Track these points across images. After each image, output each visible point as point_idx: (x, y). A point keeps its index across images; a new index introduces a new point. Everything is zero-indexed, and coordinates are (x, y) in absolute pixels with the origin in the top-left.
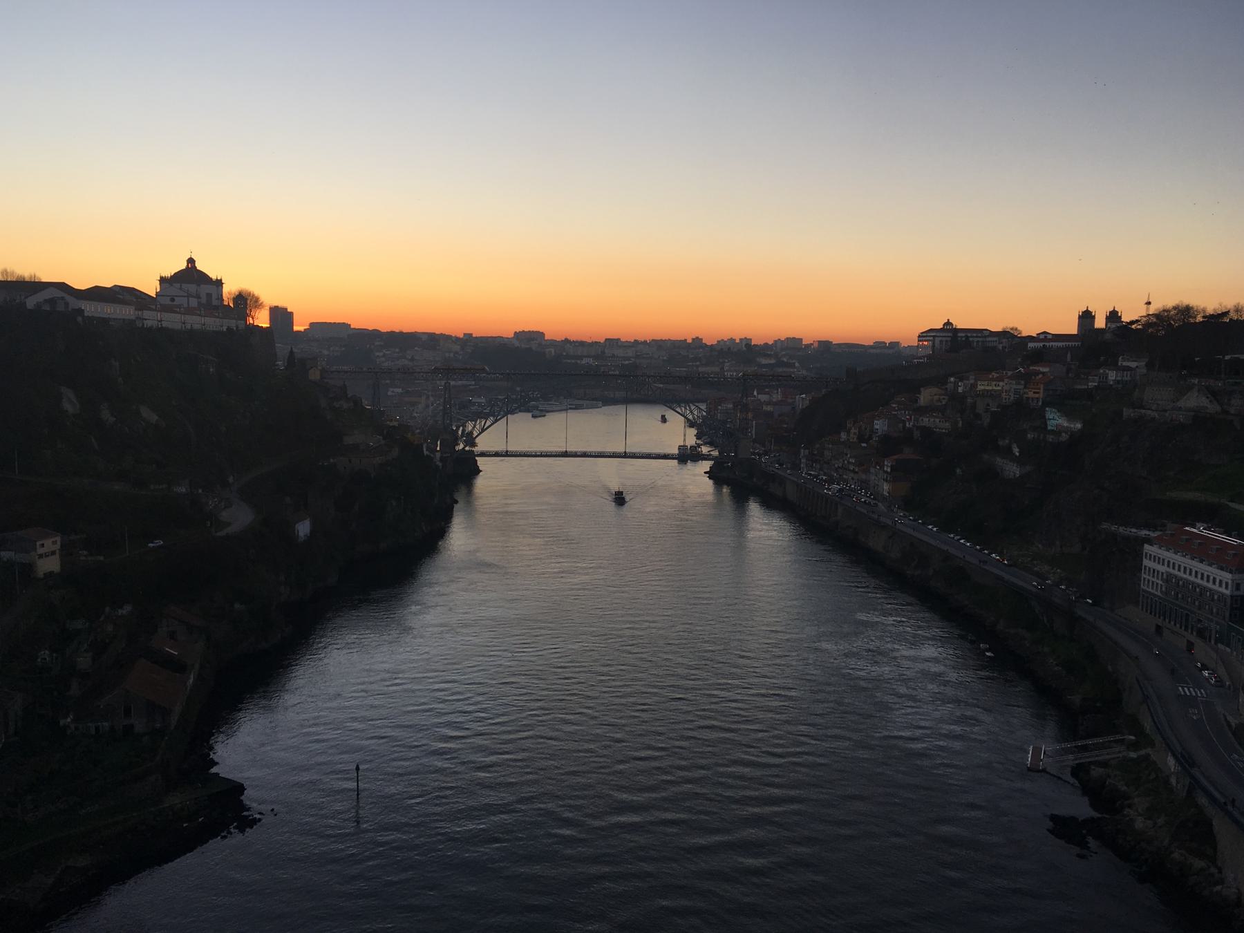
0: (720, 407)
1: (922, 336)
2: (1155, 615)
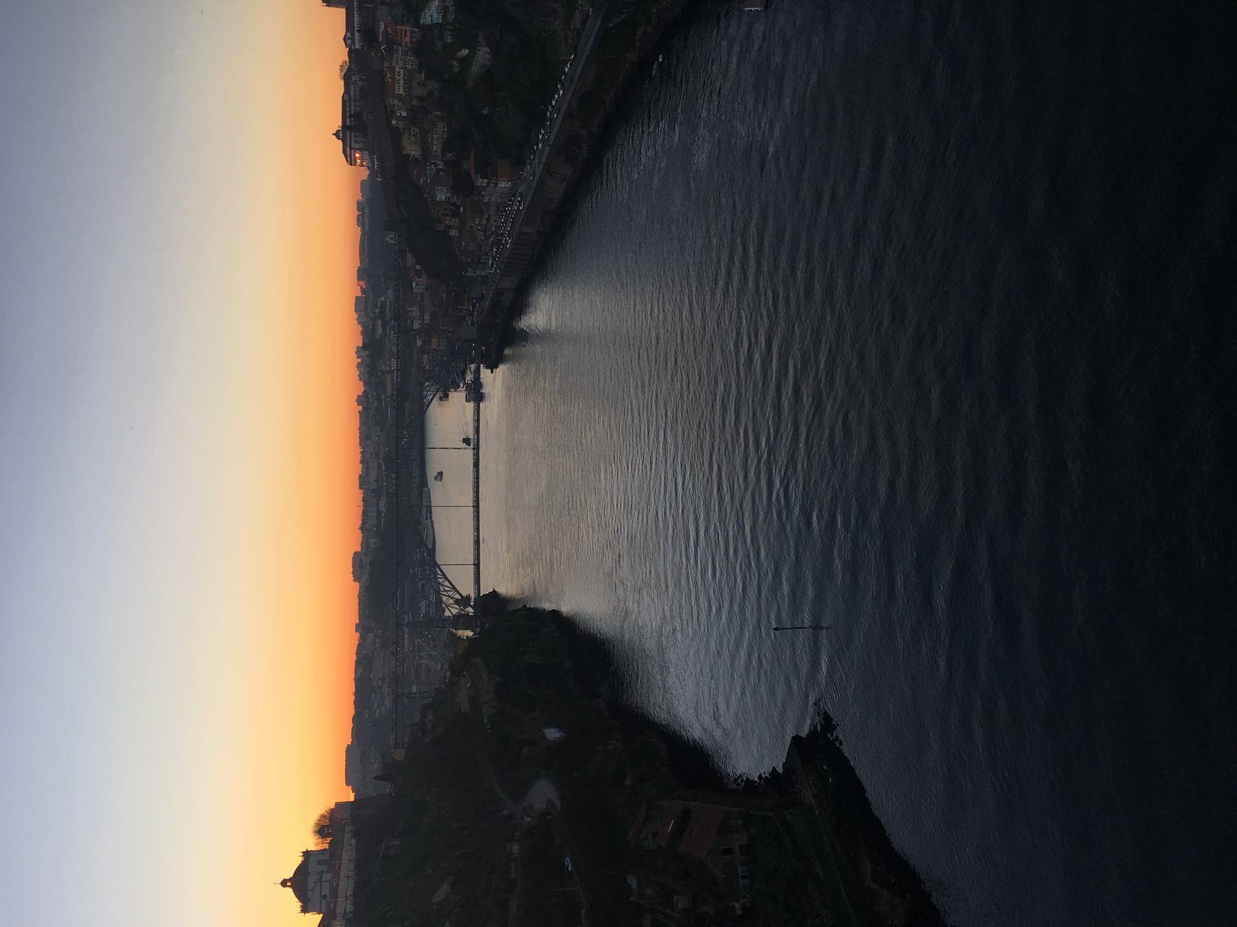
0: (427, 368)
1: (351, 161)
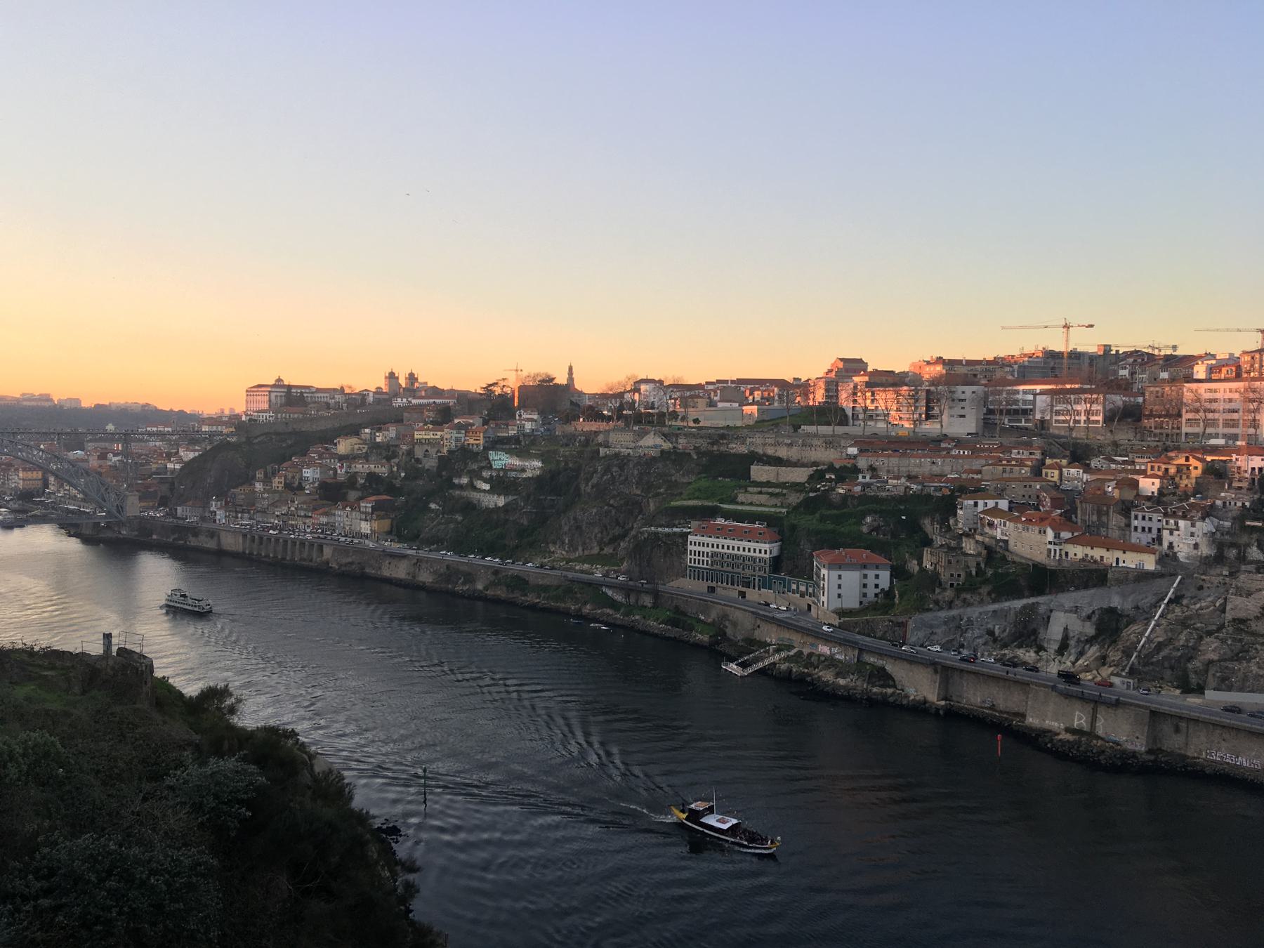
2: (703, 580)
